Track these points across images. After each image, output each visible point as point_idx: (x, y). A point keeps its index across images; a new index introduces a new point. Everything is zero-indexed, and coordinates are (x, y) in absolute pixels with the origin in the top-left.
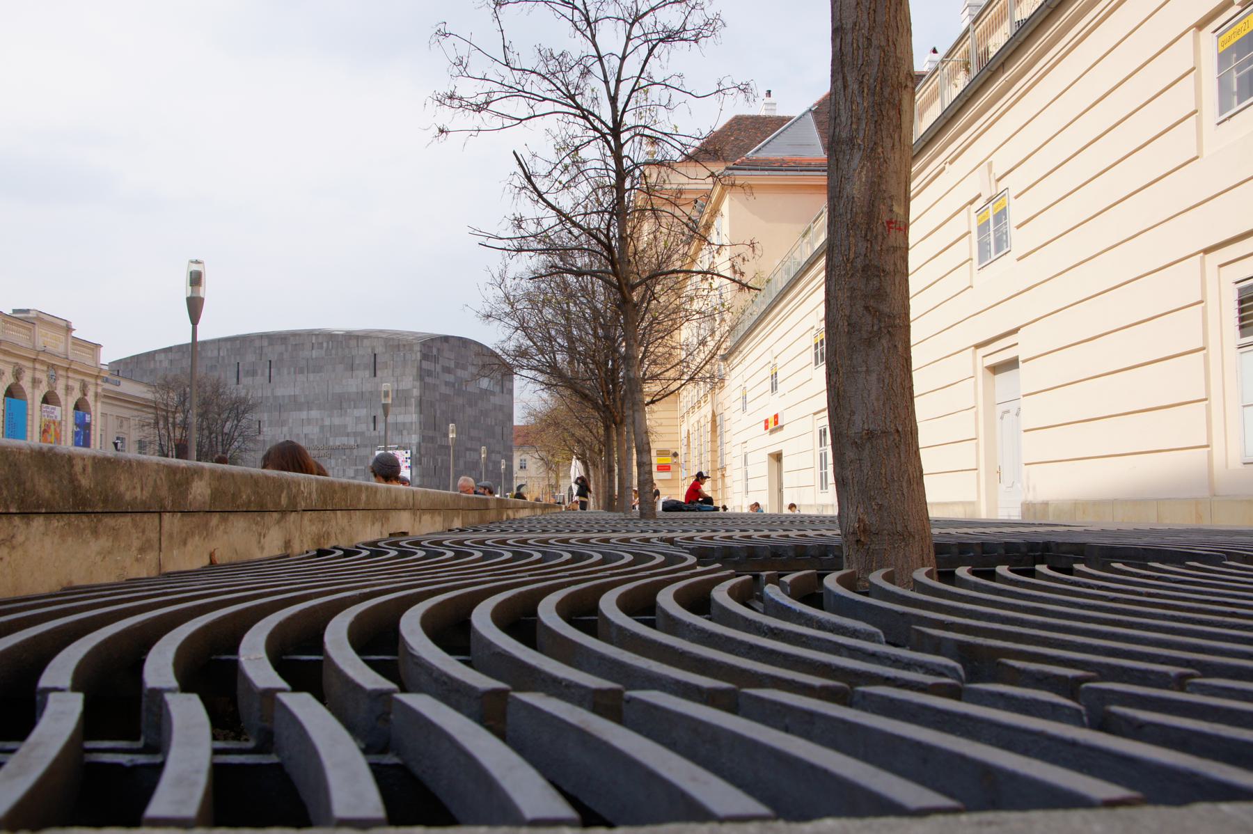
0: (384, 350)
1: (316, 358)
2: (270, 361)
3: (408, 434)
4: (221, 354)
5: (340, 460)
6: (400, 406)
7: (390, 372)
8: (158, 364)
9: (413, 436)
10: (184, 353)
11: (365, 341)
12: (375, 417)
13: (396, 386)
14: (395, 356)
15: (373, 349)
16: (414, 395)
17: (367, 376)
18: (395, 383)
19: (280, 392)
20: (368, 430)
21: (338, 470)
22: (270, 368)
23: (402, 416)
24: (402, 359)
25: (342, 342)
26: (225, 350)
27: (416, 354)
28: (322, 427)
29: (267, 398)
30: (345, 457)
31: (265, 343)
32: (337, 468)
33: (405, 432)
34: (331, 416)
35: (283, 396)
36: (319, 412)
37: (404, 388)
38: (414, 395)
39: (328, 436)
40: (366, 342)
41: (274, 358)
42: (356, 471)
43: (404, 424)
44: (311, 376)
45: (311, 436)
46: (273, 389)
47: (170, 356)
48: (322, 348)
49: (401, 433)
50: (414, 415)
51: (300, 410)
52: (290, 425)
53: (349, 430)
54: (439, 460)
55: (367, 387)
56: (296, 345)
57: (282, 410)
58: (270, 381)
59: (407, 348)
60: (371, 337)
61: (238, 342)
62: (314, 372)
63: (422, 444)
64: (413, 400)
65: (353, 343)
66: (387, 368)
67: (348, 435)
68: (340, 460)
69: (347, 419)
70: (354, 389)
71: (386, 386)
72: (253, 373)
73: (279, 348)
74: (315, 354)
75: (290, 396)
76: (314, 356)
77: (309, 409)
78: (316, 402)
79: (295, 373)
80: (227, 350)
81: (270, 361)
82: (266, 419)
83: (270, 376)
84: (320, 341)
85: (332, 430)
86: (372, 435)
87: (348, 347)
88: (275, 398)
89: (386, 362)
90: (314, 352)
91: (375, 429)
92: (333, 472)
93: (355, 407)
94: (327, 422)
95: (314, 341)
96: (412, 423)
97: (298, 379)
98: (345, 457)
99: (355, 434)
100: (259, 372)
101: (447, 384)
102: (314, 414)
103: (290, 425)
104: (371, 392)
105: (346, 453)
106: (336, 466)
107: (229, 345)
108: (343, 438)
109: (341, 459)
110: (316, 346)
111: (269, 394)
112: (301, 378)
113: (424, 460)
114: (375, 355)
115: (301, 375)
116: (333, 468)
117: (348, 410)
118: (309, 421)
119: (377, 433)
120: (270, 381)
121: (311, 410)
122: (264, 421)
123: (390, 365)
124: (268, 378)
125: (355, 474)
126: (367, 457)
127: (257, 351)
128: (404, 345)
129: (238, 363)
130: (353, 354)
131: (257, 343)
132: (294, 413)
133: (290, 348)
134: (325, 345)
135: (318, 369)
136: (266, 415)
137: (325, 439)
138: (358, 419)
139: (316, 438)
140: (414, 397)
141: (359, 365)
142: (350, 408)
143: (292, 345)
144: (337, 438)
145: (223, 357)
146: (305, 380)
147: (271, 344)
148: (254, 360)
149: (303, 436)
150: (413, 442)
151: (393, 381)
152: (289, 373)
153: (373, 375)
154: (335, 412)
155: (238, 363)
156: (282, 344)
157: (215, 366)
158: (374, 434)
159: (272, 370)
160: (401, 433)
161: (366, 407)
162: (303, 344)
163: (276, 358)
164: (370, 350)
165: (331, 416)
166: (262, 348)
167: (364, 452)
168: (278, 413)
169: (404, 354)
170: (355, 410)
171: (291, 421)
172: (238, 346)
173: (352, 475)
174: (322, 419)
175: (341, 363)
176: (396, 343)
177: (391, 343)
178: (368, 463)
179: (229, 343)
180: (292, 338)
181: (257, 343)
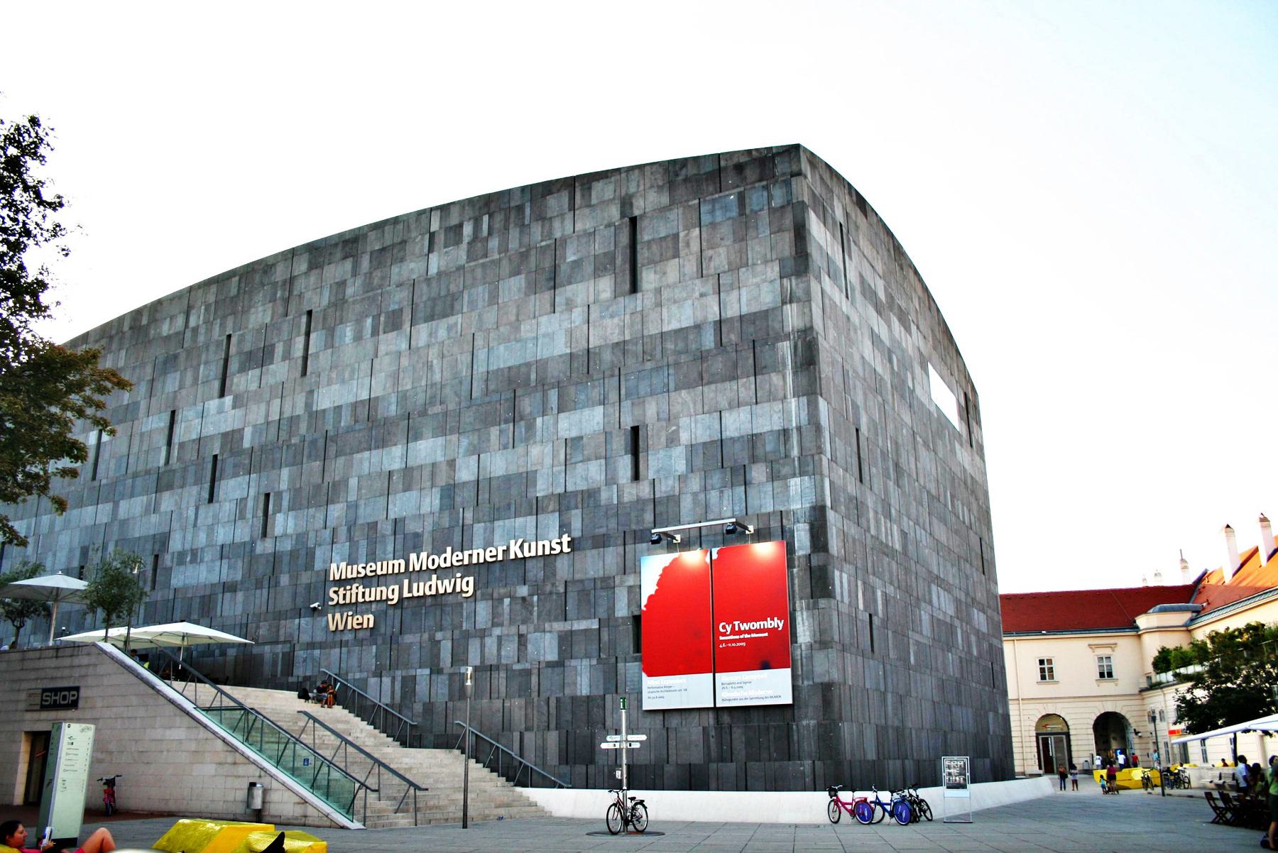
0: (665, 200)
1: (439, 274)
2: (310, 313)
3: (773, 477)
4: (192, 323)
5: (507, 601)
6: (734, 378)
7: (691, 267)
9: (795, 483)
11: (597, 186)
12: (635, 430)
13: (716, 309)
14: (704, 208)
16: (789, 328)
17: (606, 294)
18: (712, 302)
19: (327, 399)
20: (611, 480)
21: (500, 638)
22: (308, 334)
23: (744, 413)
24: (734, 212)
25: (520, 209)
28: (450, 492)
29: (294, 420)
30: (523, 591)
31: (302, 266)
32: (497, 631)
33: (758, 473)
34: (477, 451)
35: (338, 409)
36: (441, 440)
37: (745, 311)
38: (789, 328)
39: (469, 515)
40: (602, 191)
41: (319, 300)
42: (566, 640)
43: (753, 440)
45: (412, 527)
46: (311, 392)
49: (740, 476)
50: (793, 402)
51: (383, 443)
52: (352, 497)
53: (542, 488)
54: (879, 593)
56: (383, 250)
57: (332, 450)
58: (304, 373)
59: (751, 174)
62: (430, 318)
63: (831, 515)
65: (556, 203)
66: (676, 255)
67: (537, 508)
68: (507, 601)
69: (535, 451)
70: (560, 347)
71: (679, 317)
72: (261, 357)
73: (338, 270)
75: (355, 406)
76: (433, 270)
77: (412, 435)
79: (375, 332)
81: (310, 313)
82: (284, 486)
83: (305, 358)
84: (454, 220)
85: (484, 496)
86: (626, 499)
88: (315, 416)
89: (676, 236)
90: (434, 258)
91: (636, 476)
92: (483, 646)
94: (466, 473)
96: (785, 432)
97: (382, 349)
98: (523, 591)
99: (563, 502)
101: (875, 339)
102: (428, 449)
103: (352, 497)
104: (621, 347)
105: (530, 575)
106: (494, 625)
108: (520, 520)
109: (512, 597)
110: (440, 239)
111: (300, 410)
112: (392, 342)
113: (841, 580)
114: (634, 221)
116: (483, 634)
117: (539, 420)
118: (409, 476)
119: (644, 490)
120: (304, 373)
121: (418, 437)
122: (279, 494)
123: (688, 245)
124: (300, 362)
125: (561, 652)
126: (607, 584)
128: (739, 168)
130: (558, 235)
131: (280, 273)
132: (366, 454)
133: (365, 263)
134: (468, 229)
135: (442, 307)
136: (285, 472)
137: (458, 531)
138: (573, 444)
139: (429, 528)
140: (787, 337)
141: (577, 264)
144: (497, 523)
145: (195, 330)
146: (404, 346)
147: (314, 265)
148: (268, 320)
149: (386, 528)
150: (795, 506)
151: (702, 295)
152: (358, 338)
153: (627, 287)
154: (494, 431)
156: (345, 258)
158: (632, 492)
159: (313, 336)
160: (740, 476)
161: (603, 402)
162: (404, 242)
163: (325, 302)
164: (614, 212)
165: (477, 451)
166: (292, 280)
167: (595, 564)
168: (317, 464)
169: (741, 198)
170: (562, 415)
171: (353, 482)
172: (234, 292)
173: (552, 656)
174: (452, 464)
175: (518, 273)
176: (709, 167)
177: (691, 170)
178: (612, 608)
180: (372, 235)
181: (280, 273)
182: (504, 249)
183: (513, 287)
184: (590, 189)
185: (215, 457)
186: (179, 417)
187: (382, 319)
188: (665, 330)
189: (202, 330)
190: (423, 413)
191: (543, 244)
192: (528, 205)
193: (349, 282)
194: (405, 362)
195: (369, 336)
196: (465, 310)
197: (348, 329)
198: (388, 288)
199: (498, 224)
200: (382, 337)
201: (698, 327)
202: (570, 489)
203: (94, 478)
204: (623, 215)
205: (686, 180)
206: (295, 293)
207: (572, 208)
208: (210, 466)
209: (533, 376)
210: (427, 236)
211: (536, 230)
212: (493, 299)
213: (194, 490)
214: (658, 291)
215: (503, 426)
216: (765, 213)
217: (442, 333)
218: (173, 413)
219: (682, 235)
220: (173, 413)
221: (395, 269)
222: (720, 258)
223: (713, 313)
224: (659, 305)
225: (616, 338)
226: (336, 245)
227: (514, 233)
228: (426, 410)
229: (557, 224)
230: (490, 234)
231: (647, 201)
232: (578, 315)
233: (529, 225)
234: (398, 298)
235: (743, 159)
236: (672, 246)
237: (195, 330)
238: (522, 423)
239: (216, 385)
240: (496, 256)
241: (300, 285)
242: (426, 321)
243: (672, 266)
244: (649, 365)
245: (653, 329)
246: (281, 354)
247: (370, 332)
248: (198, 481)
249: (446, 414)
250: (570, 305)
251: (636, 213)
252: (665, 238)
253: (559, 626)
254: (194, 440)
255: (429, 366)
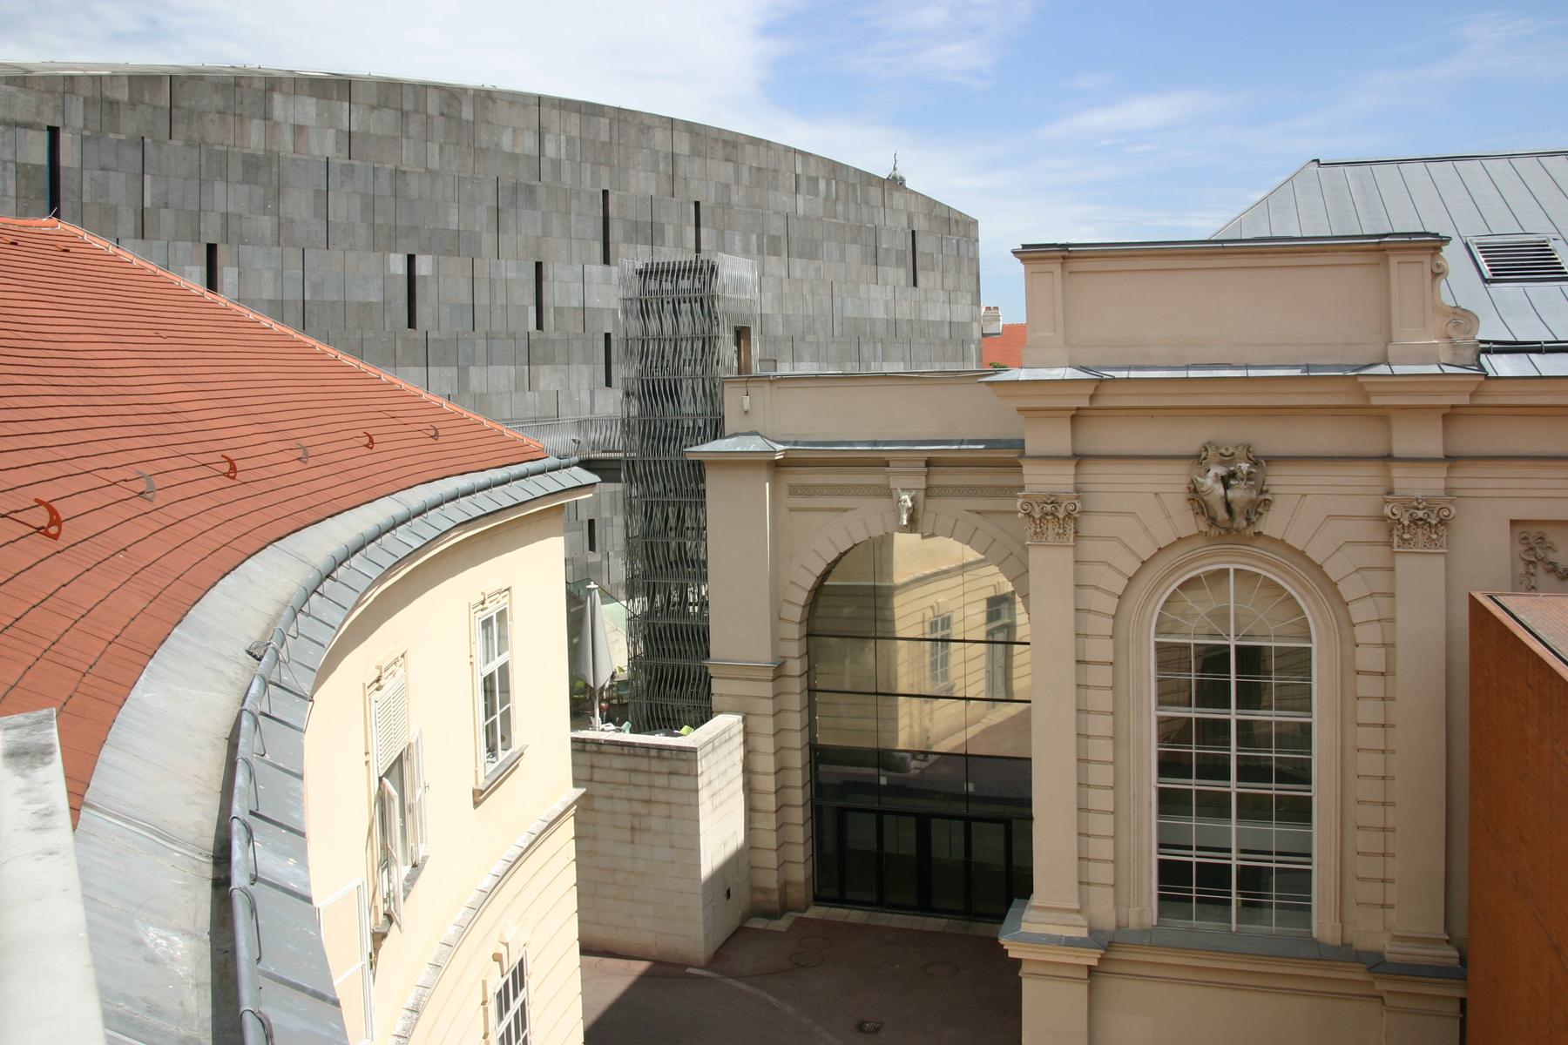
1: (806, 217)
2: (697, 204)
4: (550, 150)
8: (286, 139)
10: (404, 114)
25: (854, 186)
26: (563, 137)
31: (683, 146)
44: (798, 265)
47: (358, 119)
48: (816, 194)
55: (904, 311)
56: (760, 169)
59: (961, 227)
61: (605, 121)
62: (801, 256)
64: (973, 346)
66: (933, 270)
74: (802, 204)
78: (810, 338)
80: (570, 140)
81: (697, 204)
87: (867, 203)
93: (884, 360)
95: (799, 170)
100: (670, 231)
107: (574, 122)
110: (803, 183)
114: (913, 232)
115: (773, 259)
117: (873, 364)
121: (801, 359)
123: (937, 265)
127: (661, 166)
128: (957, 222)
129: (605, 193)
130: (877, 223)
131: (660, 138)
134: (822, 185)
143: (750, 167)
145: (557, 163)
146: (784, 274)
148: (653, 192)
155: (605, 193)
157: (530, 190)
159: (703, 231)
163: (712, 200)
169: (958, 241)
170: (884, 364)
172: (604, 137)
175: (854, 241)
176: (945, 215)
177: (937, 211)
179: (575, 118)
180: (749, 149)
181: (660, 138)
183: (854, 251)
184: (892, 194)
185: (607, 336)
186: (548, 272)
187: (765, 239)
188: (930, 319)
189: (566, 167)
190: (803, 339)
191: (869, 225)
192: (859, 186)
193: (734, 188)
194: (786, 289)
195: (756, 252)
196: (825, 258)
197: (737, 238)
198: (768, 212)
199: (842, 194)
200: (766, 257)
201: (942, 323)
203: (412, 323)
204: (909, 228)
206: (680, 173)
208: (602, 344)
210: (794, 175)
211: (865, 209)
212: (842, 259)
213: (585, 370)
214: (926, 290)
215: (854, 363)
216: (966, 259)
217: (811, 273)
218: (539, 266)
220: (539, 266)
221: (771, 195)
222: (950, 282)
225: (908, 318)
226: (717, 140)
227: (852, 207)
228: (804, 337)
230: (837, 199)
231: (920, 224)
233: (860, 205)
234: (776, 226)
237: (557, 163)
238: (864, 364)
239: (598, 247)
240: (841, 220)
241: (684, 167)
242: (798, 257)
244: (923, 340)
246: (672, 238)
247: (756, 247)
248: (588, 360)
249: (818, 344)
250: (886, 284)
252: (928, 254)
254: (576, 309)
255: (804, 300)
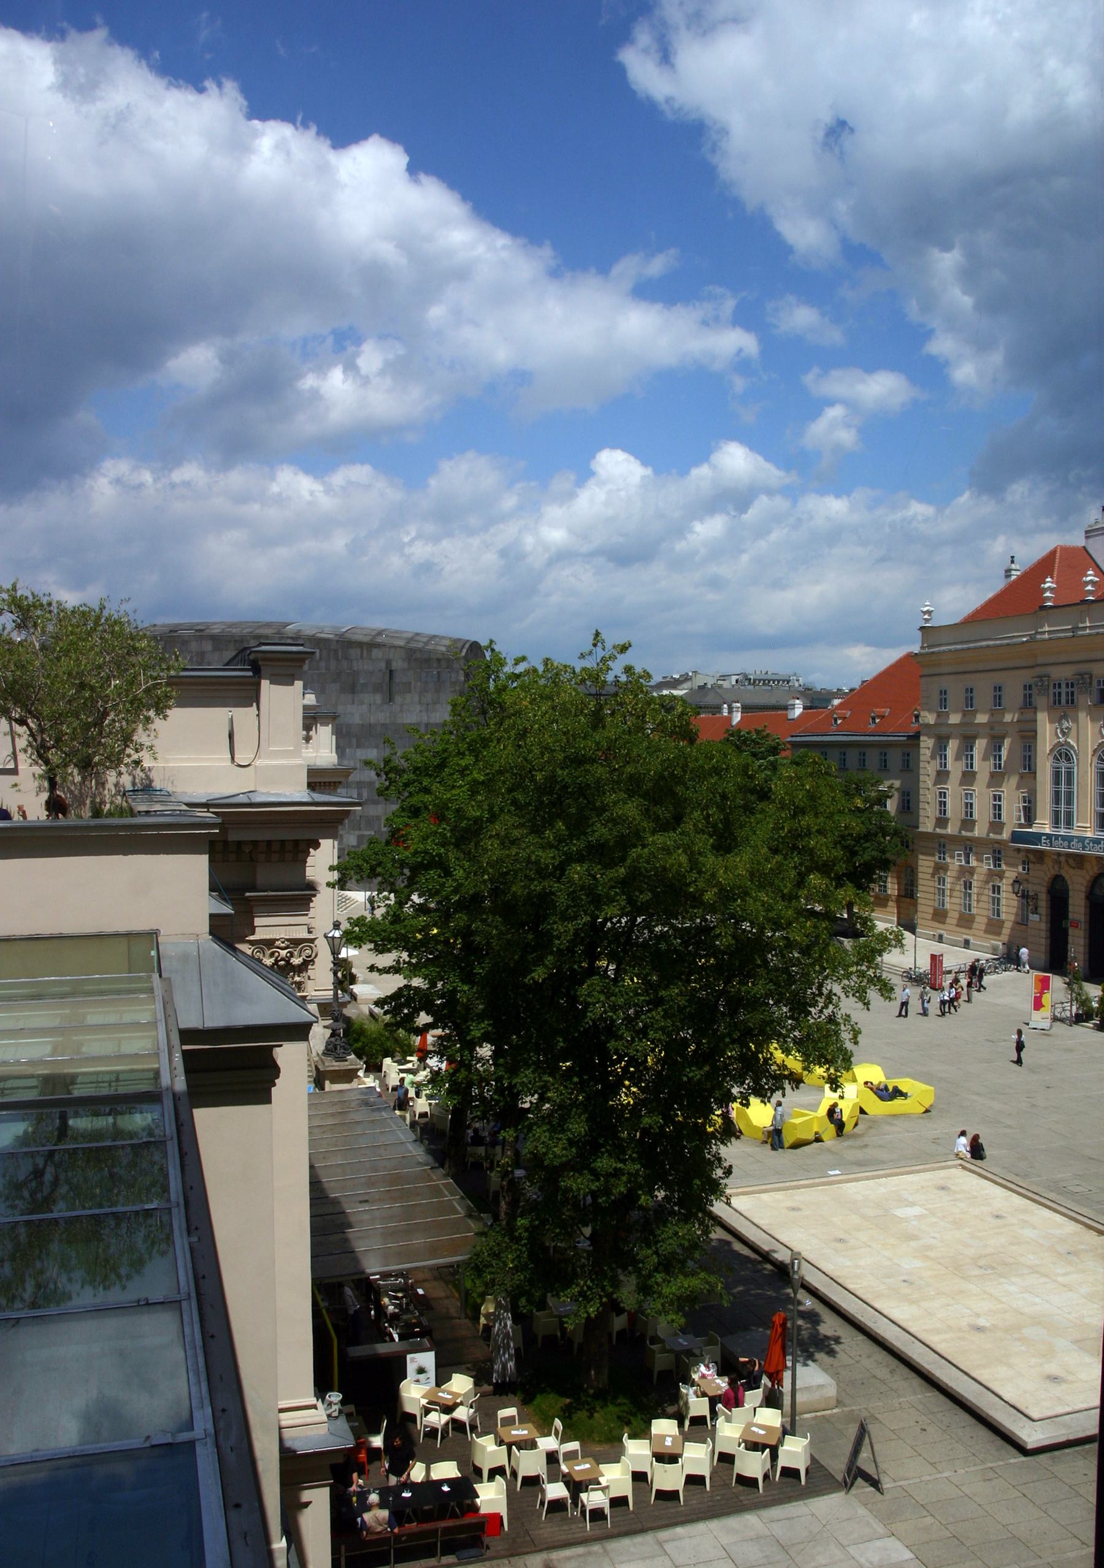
7: (416, 698)
15: (388, 662)
17: (379, 702)
24: (436, 680)
25: (336, 651)
27: (458, 672)
31: (208, 646)
40: (376, 653)
55: (380, 717)
60: (384, 645)
65: (354, 652)
70: (357, 720)
89: (410, 683)
93: (358, 746)
114: (391, 671)
117: (347, 750)
128: (439, 660)
130: (355, 669)
142: (350, 746)
147: (217, 649)
161: (377, 747)
164: (383, 665)
169: (439, 673)
177: (418, 655)
181: (194, 646)
182: (327, 668)
192: (340, 650)
201: (418, 724)
202: (362, 780)
204: (387, 668)
205: (416, 660)
207: (362, 657)
209: (344, 730)
214: (402, 706)
219: (413, 683)
222: (429, 697)
223: (425, 719)
224: (401, 711)
225: (383, 722)
229: (355, 663)
230: (321, 658)
232: (365, 707)
235: (441, 657)
236: (407, 688)
243: (408, 697)
245: (399, 721)
250: (362, 703)
251: (393, 668)
253: (357, 832)
